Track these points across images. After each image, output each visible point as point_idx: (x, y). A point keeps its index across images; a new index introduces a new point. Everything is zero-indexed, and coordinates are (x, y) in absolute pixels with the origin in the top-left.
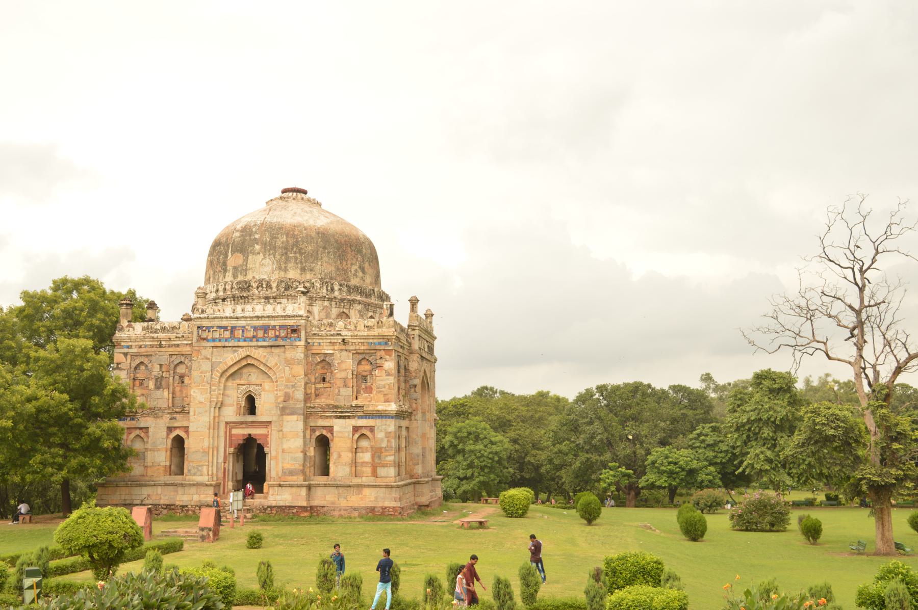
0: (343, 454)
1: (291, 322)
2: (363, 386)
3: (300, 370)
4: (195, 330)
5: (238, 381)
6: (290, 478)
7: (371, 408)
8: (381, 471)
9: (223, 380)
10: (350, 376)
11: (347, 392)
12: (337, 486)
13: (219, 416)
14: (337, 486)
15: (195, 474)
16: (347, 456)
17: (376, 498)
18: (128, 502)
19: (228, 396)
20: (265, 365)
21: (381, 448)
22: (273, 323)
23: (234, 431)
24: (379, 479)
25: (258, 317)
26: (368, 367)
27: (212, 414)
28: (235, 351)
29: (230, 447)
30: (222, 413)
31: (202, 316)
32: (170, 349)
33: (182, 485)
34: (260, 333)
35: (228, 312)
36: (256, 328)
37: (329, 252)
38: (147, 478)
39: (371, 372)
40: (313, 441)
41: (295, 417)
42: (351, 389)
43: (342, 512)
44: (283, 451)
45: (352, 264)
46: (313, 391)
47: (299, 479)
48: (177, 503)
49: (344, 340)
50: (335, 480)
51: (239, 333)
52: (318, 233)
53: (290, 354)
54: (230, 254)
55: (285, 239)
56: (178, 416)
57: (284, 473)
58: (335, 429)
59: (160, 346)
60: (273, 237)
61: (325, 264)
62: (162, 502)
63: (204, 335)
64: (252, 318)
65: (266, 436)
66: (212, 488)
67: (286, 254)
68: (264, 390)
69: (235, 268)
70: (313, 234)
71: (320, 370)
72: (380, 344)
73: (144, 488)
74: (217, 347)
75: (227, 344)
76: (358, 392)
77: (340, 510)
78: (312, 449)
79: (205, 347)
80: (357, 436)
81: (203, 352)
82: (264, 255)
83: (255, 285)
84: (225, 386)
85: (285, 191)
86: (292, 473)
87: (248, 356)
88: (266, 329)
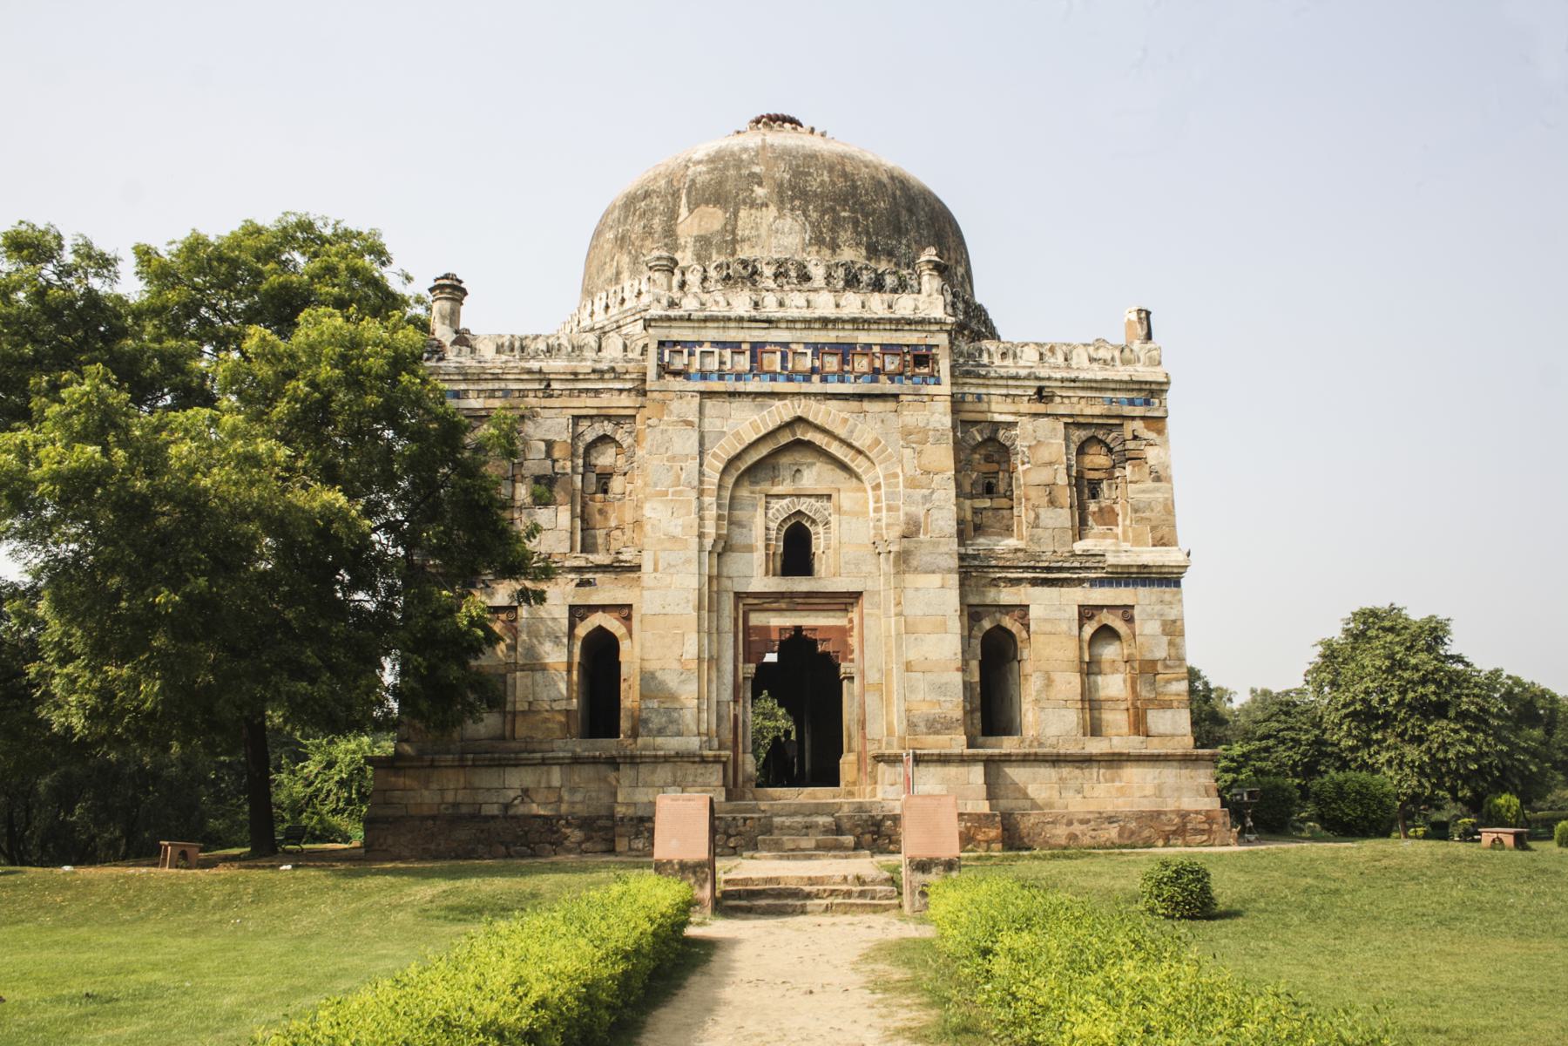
0: (1057, 676)
1: (911, 338)
2: (1093, 506)
3: (942, 457)
4: (653, 348)
5: (766, 487)
6: (931, 739)
7: (1124, 560)
8: (1158, 720)
9: (730, 481)
10: (1062, 479)
11: (1062, 517)
12: (1056, 760)
13: (719, 576)
14: (1056, 760)
15: (660, 732)
16: (1069, 684)
17: (1159, 789)
18: (464, 810)
19: (740, 525)
20: (843, 441)
21: (1154, 662)
22: (863, 338)
23: (756, 619)
24: (1156, 740)
25: (825, 322)
26: (1102, 460)
27: (706, 571)
28: (762, 407)
29: (747, 661)
30: (725, 572)
31: (673, 313)
32: (575, 402)
33: (634, 761)
34: (832, 363)
35: (741, 303)
36: (818, 349)
37: (919, 222)
38: (513, 745)
39: (1110, 472)
40: (976, 644)
41: (936, 579)
42: (1066, 512)
43: (1077, 828)
44: (908, 667)
45: (957, 262)
46: (969, 515)
47: (956, 742)
48: (621, 811)
49: (1040, 390)
50: (1041, 745)
51: (773, 362)
52: (892, 178)
53: (913, 416)
54: (684, 211)
55: (826, 178)
56: (598, 576)
57: (912, 726)
58: (1034, 612)
59: (548, 392)
60: (797, 173)
61: (914, 246)
62: (564, 808)
63: (679, 363)
64: (808, 323)
65: (844, 632)
66: (719, 767)
67: (833, 209)
68: (839, 510)
69: (704, 242)
70: (885, 179)
71: (984, 461)
72: (1131, 402)
73: (523, 769)
74: (705, 395)
75: (740, 386)
76: (1083, 521)
77: (1070, 823)
78: (974, 665)
79: (681, 394)
80: (1089, 630)
81: (675, 405)
82: (780, 209)
83: (768, 271)
84: (732, 498)
85: (758, 121)
86: (936, 726)
87: (799, 420)
88: (845, 351)
